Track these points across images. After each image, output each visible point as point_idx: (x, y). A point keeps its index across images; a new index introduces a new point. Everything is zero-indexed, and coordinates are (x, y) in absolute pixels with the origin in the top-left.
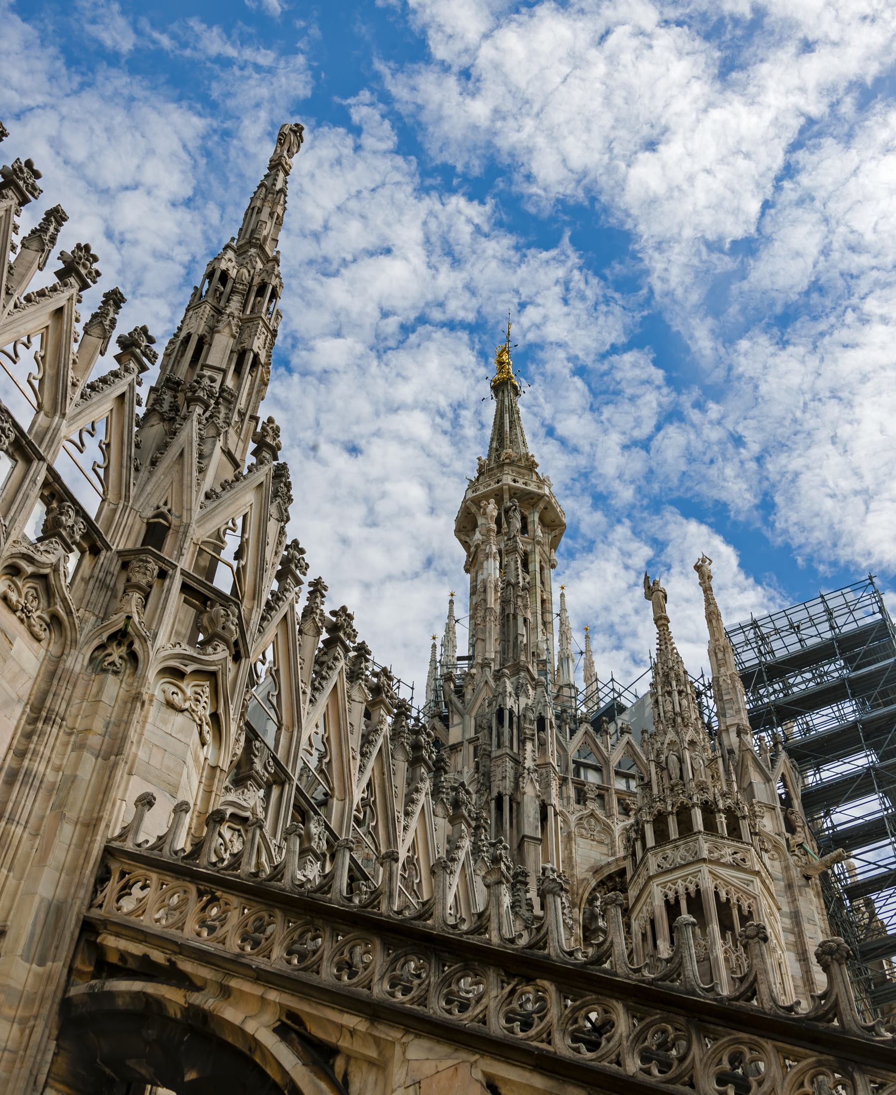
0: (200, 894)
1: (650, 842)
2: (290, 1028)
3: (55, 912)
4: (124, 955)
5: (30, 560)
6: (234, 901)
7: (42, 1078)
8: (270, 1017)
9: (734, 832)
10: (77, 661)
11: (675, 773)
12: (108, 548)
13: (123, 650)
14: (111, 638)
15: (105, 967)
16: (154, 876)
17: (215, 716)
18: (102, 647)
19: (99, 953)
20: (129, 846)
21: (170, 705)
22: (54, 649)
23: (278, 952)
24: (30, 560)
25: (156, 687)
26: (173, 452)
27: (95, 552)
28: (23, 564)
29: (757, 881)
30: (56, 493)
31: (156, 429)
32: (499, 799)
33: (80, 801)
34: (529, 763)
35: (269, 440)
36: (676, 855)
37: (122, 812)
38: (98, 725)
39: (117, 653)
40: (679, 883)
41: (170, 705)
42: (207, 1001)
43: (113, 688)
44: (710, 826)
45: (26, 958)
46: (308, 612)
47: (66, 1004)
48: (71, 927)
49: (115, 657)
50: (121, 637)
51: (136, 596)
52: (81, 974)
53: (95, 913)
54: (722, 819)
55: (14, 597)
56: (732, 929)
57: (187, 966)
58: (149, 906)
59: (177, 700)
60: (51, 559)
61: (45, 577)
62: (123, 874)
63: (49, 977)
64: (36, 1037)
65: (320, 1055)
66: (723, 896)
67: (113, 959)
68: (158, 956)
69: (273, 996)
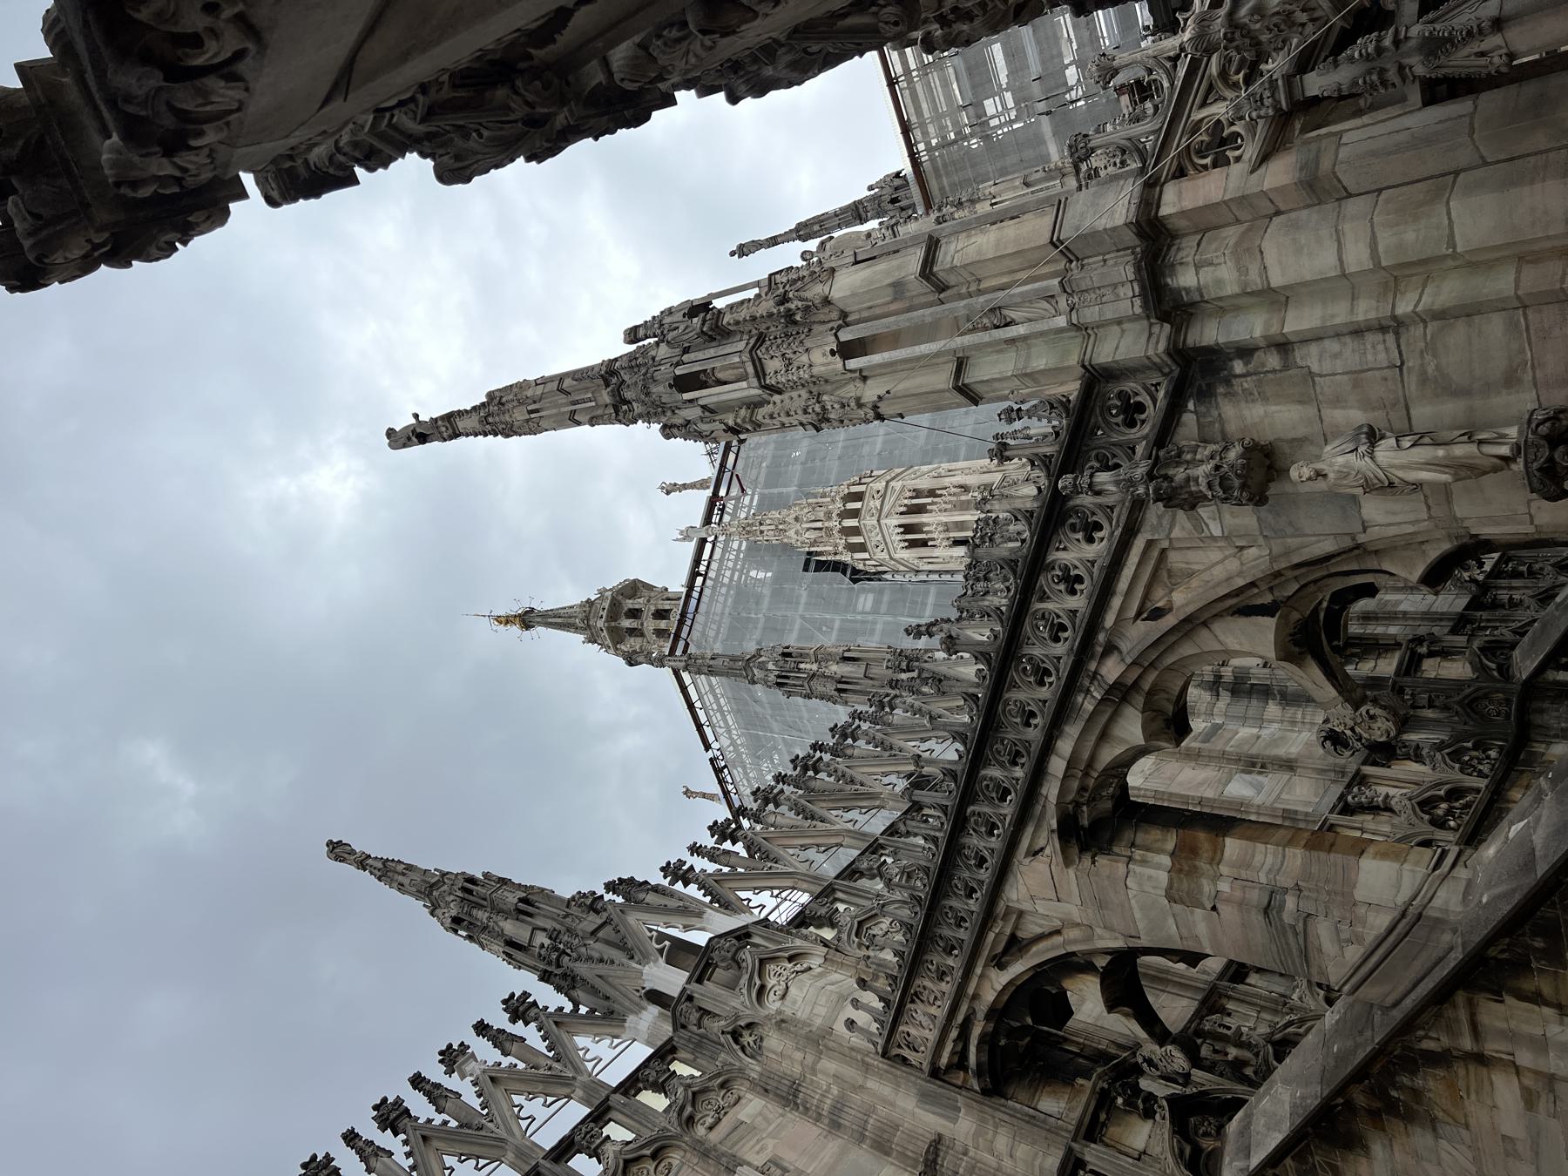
0: (913, 1001)
1: (866, 555)
2: (1000, 963)
3: (925, 1098)
4: (953, 1053)
5: (682, 1108)
6: (918, 982)
7: (1031, 1111)
8: (993, 973)
9: (859, 497)
10: (754, 1068)
11: (817, 533)
12: (671, 1039)
13: (746, 1033)
14: (737, 1042)
15: (960, 1062)
16: (901, 1028)
17: (790, 959)
18: (743, 1049)
19: (949, 1067)
20: (881, 1041)
21: (783, 997)
22: (747, 1083)
23: (950, 962)
24: (682, 1108)
25: (772, 1004)
26: (598, 983)
27: (674, 1050)
28: (686, 1113)
29: (892, 484)
30: (632, 1084)
31: (579, 994)
32: (839, 691)
33: (850, 1073)
34: (815, 667)
35: (588, 902)
36: (873, 538)
37: (856, 1040)
38: (798, 1055)
39: (747, 1039)
40: (896, 538)
41: (783, 997)
42: (982, 1008)
43: (774, 1041)
44: (855, 514)
45: (955, 1120)
46: (712, 859)
47: (985, 1092)
48: (933, 1087)
49: (751, 1040)
50: (736, 1035)
51: (706, 1021)
52: (965, 1081)
53: (926, 1066)
54: (852, 506)
55: (709, 1121)
56: (924, 505)
57: (960, 1018)
58: (923, 1026)
59: (780, 989)
60: (681, 1090)
61: (694, 1094)
62: (899, 1046)
63: (967, 1105)
64: (1006, 1118)
65: (1015, 946)
66: (903, 509)
67: (956, 1059)
68: (954, 1034)
69: (978, 970)
